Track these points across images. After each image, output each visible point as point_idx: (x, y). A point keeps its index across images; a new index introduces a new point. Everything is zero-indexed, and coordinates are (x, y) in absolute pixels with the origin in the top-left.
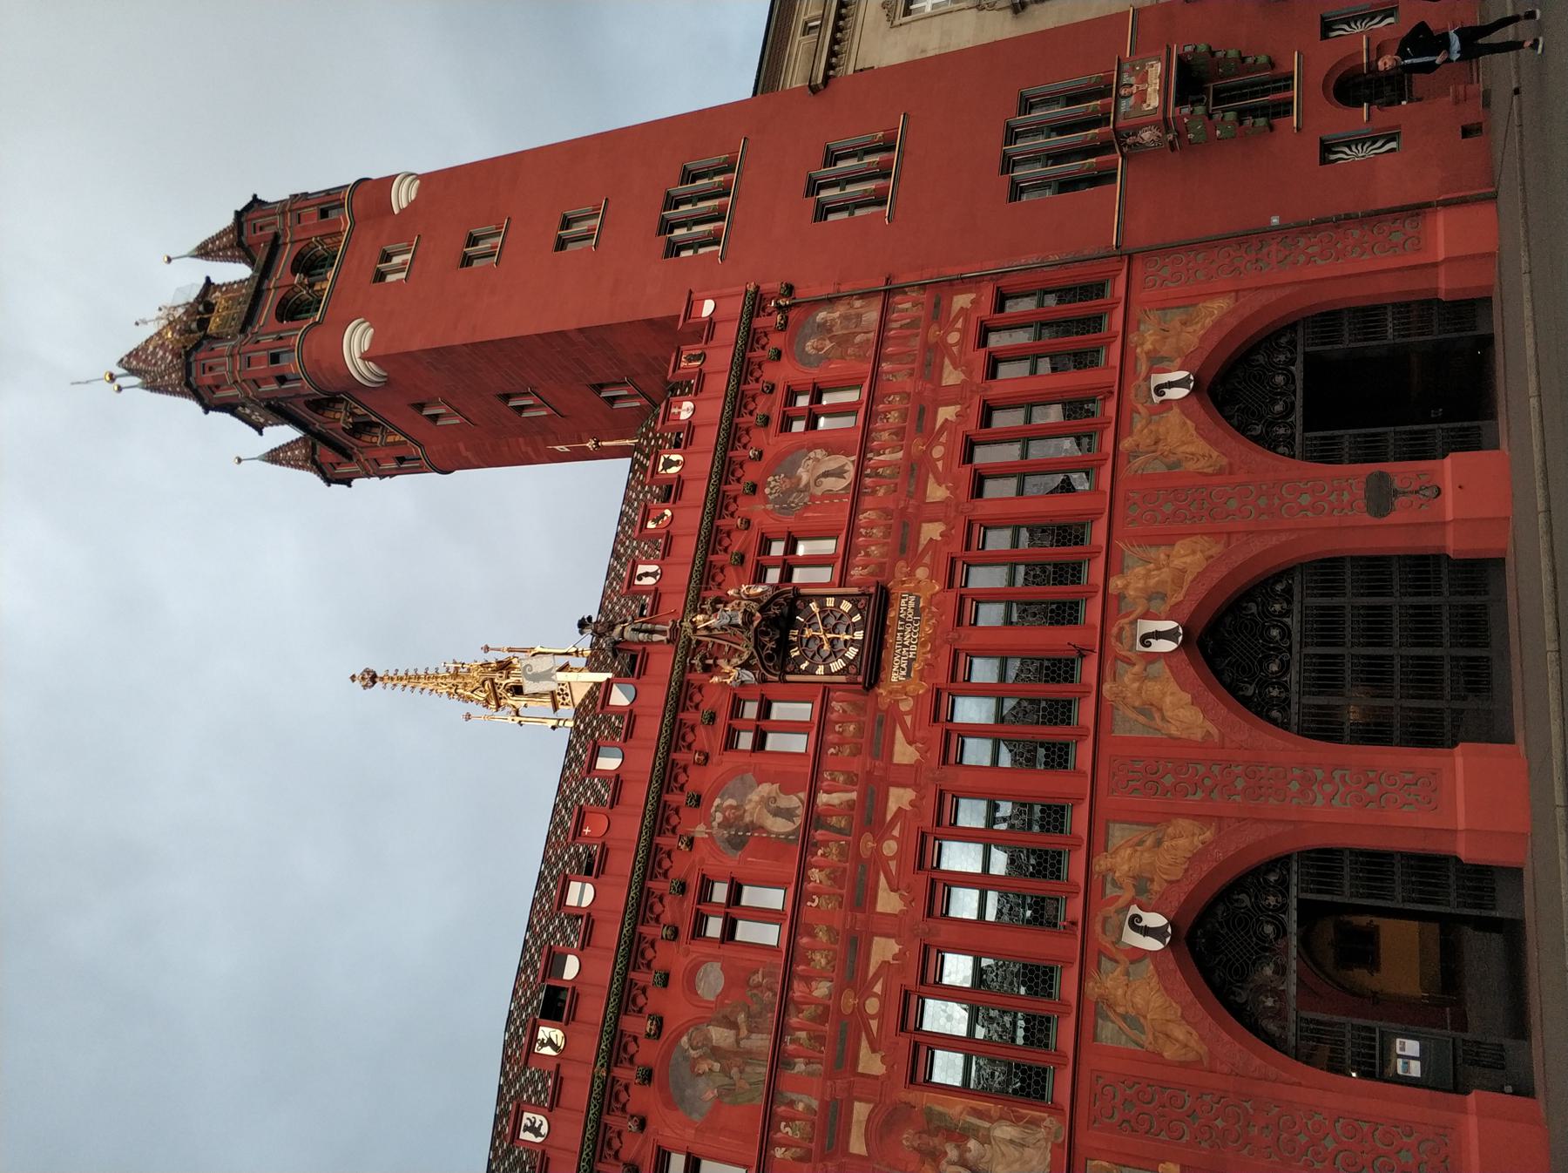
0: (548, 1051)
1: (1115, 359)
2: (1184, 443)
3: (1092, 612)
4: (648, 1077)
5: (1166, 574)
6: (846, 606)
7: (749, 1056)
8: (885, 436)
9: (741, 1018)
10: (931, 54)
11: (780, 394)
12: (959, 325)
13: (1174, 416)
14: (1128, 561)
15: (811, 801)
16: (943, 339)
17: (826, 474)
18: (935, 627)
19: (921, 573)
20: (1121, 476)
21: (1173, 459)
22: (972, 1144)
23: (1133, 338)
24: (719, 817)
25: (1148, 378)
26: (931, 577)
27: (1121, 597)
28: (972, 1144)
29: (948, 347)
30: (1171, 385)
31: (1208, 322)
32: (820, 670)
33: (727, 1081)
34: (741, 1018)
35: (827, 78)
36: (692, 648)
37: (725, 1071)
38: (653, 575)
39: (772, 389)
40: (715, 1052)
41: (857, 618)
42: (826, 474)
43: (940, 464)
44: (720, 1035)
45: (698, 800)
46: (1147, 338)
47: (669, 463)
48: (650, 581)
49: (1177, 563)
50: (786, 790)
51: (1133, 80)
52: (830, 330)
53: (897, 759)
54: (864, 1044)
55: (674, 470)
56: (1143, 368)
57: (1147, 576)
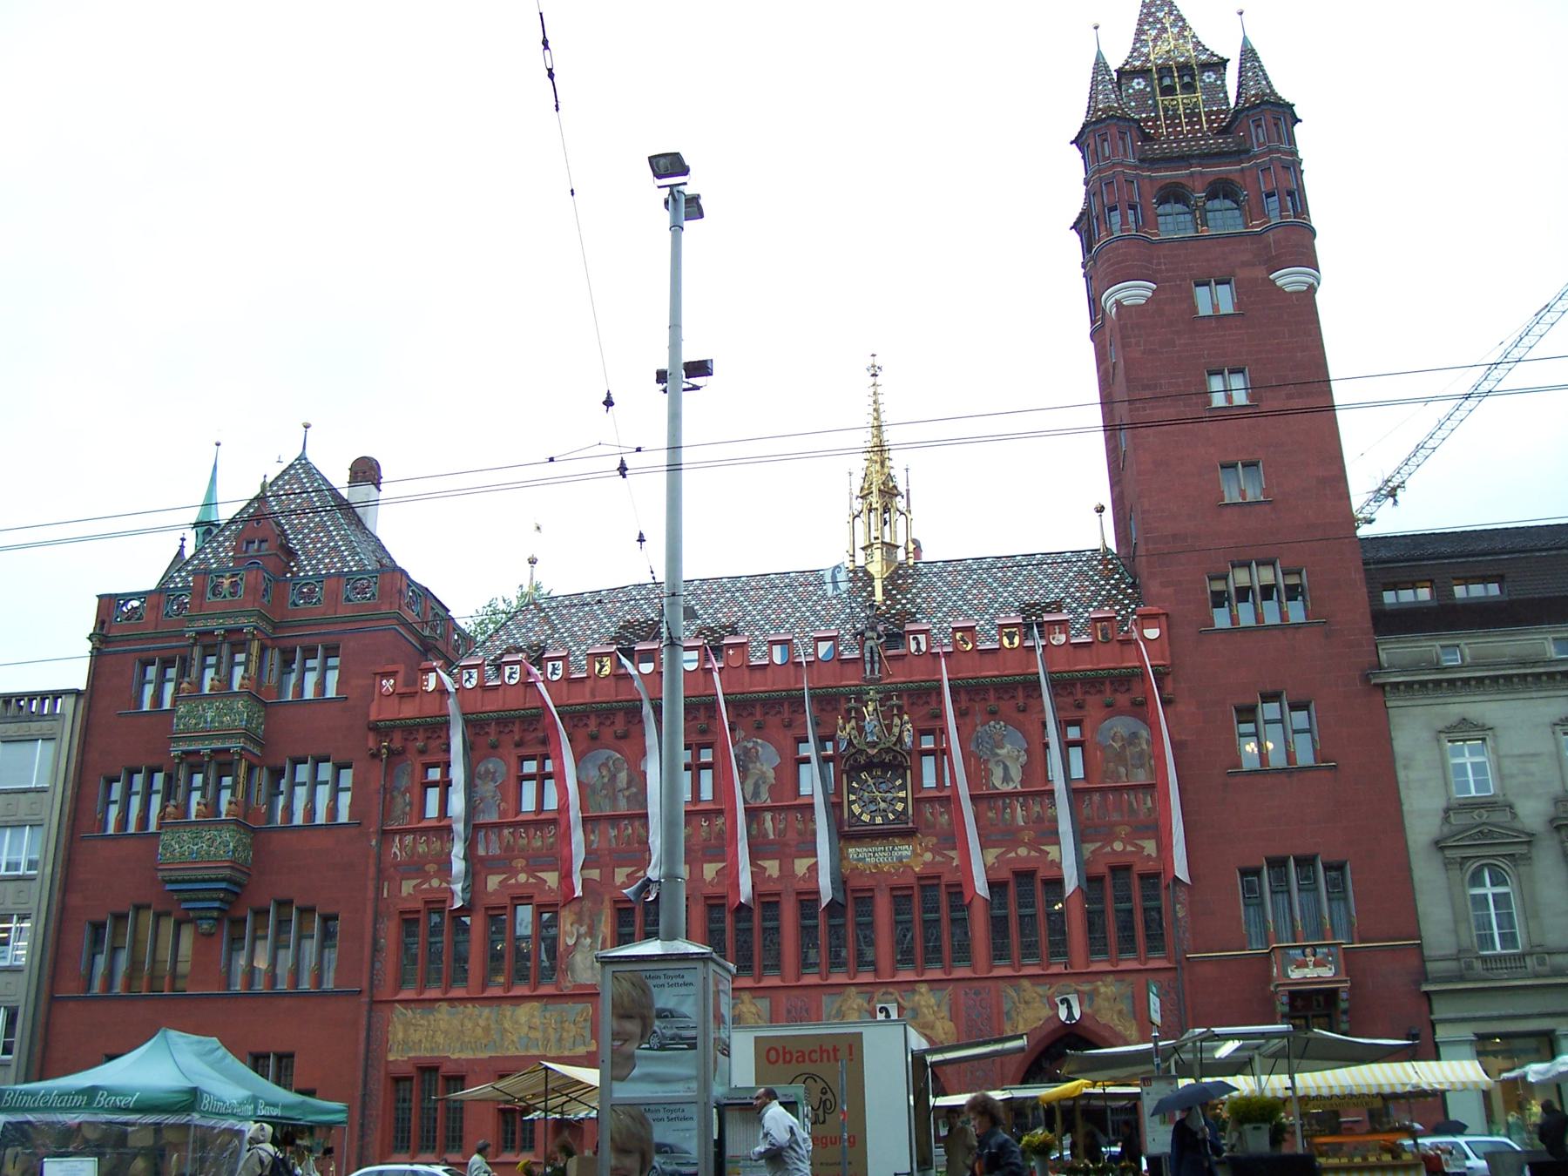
0: (598, 666)
1: (1094, 968)
2: (1025, 1020)
3: (906, 975)
4: (594, 738)
5: (931, 1018)
6: (900, 807)
7: (614, 800)
8: (1037, 808)
9: (634, 790)
10: (1401, 775)
11: (1077, 715)
12: (1129, 848)
13: (1047, 1012)
14: (939, 994)
15: (769, 809)
16: (1117, 838)
17: (1006, 768)
18: (889, 873)
19: (928, 856)
20: (1001, 984)
21: (1014, 1014)
22: (588, 940)
23: (1110, 978)
24: (750, 745)
25: (1077, 992)
26: (925, 864)
27: (914, 991)
28: (588, 940)
29: (1110, 843)
30: (1070, 1008)
31: (1120, 1028)
32: (853, 797)
33: (599, 786)
34: (634, 790)
35: (1383, 686)
36: (860, 698)
37: (604, 786)
38: (918, 649)
39: (1080, 707)
40: (613, 778)
41: (891, 816)
42: (1006, 768)
43: (1013, 855)
44: (623, 777)
45: (759, 727)
46: (1107, 988)
47: (1011, 637)
48: (913, 647)
49: (938, 1024)
50: (772, 789)
51: (1319, 956)
52: (1130, 744)
53: (797, 861)
54: (630, 870)
55: (1006, 642)
56: (1086, 987)
57: (929, 1007)
